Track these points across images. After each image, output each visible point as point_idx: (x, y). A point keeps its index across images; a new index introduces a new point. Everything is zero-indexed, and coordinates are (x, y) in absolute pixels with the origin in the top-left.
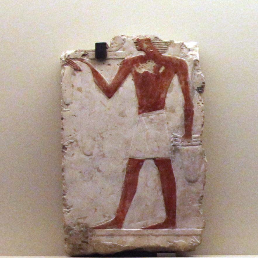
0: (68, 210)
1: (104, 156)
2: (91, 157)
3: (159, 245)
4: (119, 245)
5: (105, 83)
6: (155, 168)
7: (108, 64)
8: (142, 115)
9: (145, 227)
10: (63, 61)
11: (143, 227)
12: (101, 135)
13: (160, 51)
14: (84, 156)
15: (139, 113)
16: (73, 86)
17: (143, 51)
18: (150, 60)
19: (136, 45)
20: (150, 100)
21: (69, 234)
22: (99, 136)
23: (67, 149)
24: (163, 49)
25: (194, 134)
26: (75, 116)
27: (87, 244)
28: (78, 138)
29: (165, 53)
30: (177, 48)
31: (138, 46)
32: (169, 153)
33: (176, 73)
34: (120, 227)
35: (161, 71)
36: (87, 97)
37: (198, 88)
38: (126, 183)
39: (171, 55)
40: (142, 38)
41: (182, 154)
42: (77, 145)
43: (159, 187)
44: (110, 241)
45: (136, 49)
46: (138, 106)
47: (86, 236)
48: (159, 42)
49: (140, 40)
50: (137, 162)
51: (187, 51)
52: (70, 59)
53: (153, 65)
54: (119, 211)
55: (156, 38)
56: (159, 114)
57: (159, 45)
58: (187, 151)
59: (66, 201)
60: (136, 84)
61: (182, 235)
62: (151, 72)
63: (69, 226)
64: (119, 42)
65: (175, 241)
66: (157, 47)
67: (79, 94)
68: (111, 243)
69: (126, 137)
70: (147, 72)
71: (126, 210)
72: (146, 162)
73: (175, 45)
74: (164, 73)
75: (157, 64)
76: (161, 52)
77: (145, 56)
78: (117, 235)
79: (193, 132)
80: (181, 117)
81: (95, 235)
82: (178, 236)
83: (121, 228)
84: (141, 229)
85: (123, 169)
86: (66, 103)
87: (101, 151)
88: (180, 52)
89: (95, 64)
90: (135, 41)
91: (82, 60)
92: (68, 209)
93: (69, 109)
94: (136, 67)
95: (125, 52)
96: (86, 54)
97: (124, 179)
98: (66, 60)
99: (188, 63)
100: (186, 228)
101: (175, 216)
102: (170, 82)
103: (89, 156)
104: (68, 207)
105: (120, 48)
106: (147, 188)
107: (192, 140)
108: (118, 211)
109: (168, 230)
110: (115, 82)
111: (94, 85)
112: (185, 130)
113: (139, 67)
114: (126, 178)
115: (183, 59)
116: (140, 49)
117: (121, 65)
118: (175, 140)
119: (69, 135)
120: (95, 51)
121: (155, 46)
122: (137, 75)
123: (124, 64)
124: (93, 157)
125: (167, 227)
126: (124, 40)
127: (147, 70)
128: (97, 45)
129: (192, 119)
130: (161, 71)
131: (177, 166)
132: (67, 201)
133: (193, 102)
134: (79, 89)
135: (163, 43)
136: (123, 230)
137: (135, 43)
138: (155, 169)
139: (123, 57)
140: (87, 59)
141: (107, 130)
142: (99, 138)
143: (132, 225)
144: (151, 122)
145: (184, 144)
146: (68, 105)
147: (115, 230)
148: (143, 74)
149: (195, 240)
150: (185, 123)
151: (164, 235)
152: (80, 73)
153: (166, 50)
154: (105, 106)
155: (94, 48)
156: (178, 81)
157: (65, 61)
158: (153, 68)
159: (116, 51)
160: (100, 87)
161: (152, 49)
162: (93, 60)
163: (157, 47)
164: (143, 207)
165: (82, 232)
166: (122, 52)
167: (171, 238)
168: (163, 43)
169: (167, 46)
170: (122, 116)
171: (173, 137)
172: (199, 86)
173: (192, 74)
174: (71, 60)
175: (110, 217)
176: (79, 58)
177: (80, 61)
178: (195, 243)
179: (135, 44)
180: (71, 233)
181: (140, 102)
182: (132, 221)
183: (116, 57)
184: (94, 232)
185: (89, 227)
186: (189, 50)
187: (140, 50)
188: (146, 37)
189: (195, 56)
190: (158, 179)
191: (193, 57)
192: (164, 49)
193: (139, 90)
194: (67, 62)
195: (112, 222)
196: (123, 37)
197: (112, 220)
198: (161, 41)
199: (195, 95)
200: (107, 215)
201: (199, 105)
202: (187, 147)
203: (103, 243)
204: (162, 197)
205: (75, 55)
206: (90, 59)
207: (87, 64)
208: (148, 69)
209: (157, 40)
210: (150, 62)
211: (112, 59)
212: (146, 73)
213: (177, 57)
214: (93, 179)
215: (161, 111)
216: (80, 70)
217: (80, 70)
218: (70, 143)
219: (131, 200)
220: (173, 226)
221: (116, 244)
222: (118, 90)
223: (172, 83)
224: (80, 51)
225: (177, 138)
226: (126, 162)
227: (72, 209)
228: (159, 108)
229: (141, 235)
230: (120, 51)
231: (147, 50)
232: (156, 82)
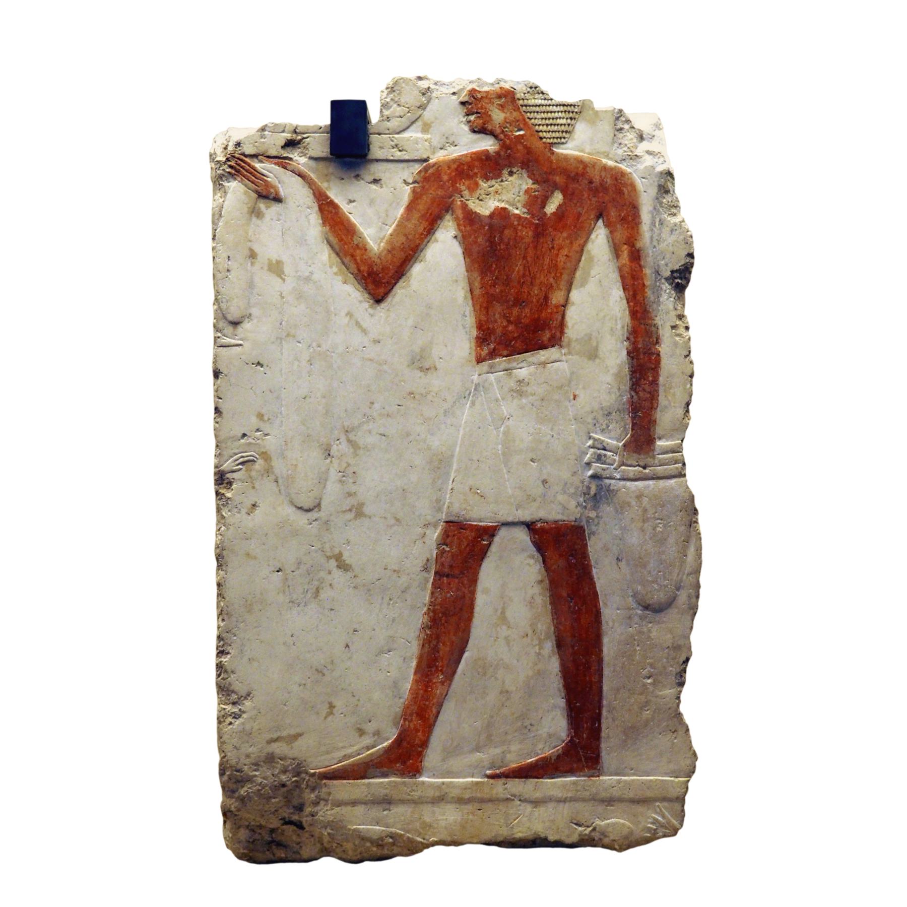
0: (235, 710)
1: (358, 511)
2: (314, 515)
3: (543, 836)
4: (408, 838)
5: (363, 248)
6: (532, 557)
7: (371, 178)
8: (491, 367)
9: (498, 772)
10: (218, 162)
11: (489, 772)
12: (352, 436)
13: (548, 135)
14: (290, 511)
15: (480, 360)
16: (253, 255)
17: (492, 133)
18: (515, 170)
19: (468, 114)
20: (515, 311)
21: (237, 795)
22: (343, 439)
23: (234, 486)
24: (556, 128)
25: (660, 439)
26: (259, 364)
27: (299, 832)
28: (271, 443)
29: (563, 143)
30: (606, 127)
31: (472, 118)
32: (579, 505)
33: (599, 216)
34: (416, 771)
35: (551, 208)
36: (300, 296)
37: (672, 272)
38: (434, 611)
39: (582, 151)
40: (486, 89)
41: (623, 507)
42: (268, 471)
43: (545, 625)
44: (378, 824)
45: (466, 128)
46: (475, 333)
47: (295, 802)
48: (543, 102)
49: (479, 96)
50: (470, 535)
51: (635, 140)
52: (242, 157)
53: (525, 187)
54: (411, 715)
55: (534, 89)
56: (544, 364)
57: (543, 115)
58: (639, 497)
59: (230, 677)
60: (467, 253)
61: (621, 800)
62: (517, 212)
63: (238, 767)
64: (411, 97)
65: (598, 822)
66: (536, 122)
67: (270, 285)
68: (383, 830)
69: (435, 442)
70: (504, 209)
71: (434, 711)
72: (503, 533)
73: (597, 115)
74: (560, 215)
75: (536, 182)
76: (551, 141)
77: (498, 153)
78: (402, 802)
79: (659, 430)
80: (618, 375)
81: (326, 801)
82: (610, 801)
83: (414, 776)
84: (486, 780)
85: (425, 561)
86: (230, 318)
87: (349, 494)
88: (613, 142)
89: (326, 177)
90: (462, 99)
91: (282, 161)
92: (234, 703)
93: (241, 340)
94: (466, 193)
95: (429, 136)
96: (299, 142)
97: (427, 599)
98: (228, 160)
99: (640, 184)
100: (634, 775)
101: (599, 729)
102: (582, 250)
103: (309, 510)
104: (234, 697)
105: (413, 123)
106: (504, 627)
107: (654, 457)
108: (406, 715)
109: (574, 783)
110: (398, 245)
111: (325, 255)
112: (634, 424)
113: (479, 192)
114: (432, 593)
115: (623, 166)
116: (425, 224)
117: (416, 185)
118: (599, 458)
119: (240, 435)
120: (329, 130)
121: (531, 119)
122: (470, 219)
123: (426, 179)
124: (322, 514)
125: (570, 772)
126: (426, 92)
127: (503, 205)
128: (338, 107)
129: (655, 382)
130: (551, 208)
131: (606, 549)
132: (232, 676)
133: (658, 321)
134: (276, 268)
135: (555, 108)
136: (423, 783)
137: (463, 103)
138: (532, 562)
139: (425, 156)
140: (303, 160)
141: (368, 418)
142: (344, 447)
143: (456, 763)
144: (521, 394)
145: (628, 471)
146: (235, 324)
147: (395, 782)
148: (492, 216)
149: (664, 817)
150: (632, 397)
151: (564, 801)
152: (275, 208)
153: (566, 132)
154: (364, 331)
155: (325, 119)
156: (605, 241)
157: (225, 163)
158: (523, 198)
159: (398, 133)
160: (347, 260)
161: (520, 130)
162: (321, 165)
163: (537, 119)
164: (492, 697)
165: (284, 789)
166: (419, 135)
167: (585, 810)
168: (555, 108)
169: (571, 119)
170: (421, 369)
171: (590, 447)
172: (676, 267)
173: (653, 224)
174: (247, 160)
175: (377, 733)
176: (273, 152)
177: (275, 164)
178: (662, 826)
179: (462, 110)
180: (242, 792)
181: (483, 318)
182: (451, 751)
183: (399, 153)
184: (324, 790)
185: (307, 773)
186: (641, 138)
187: (481, 130)
188: (497, 86)
189: (662, 160)
190: (539, 596)
191: (656, 160)
192: (559, 128)
193: (476, 275)
194: (231, 167)
195: (388, 750)
196: (424, 84)
197: (386, 744)
198: (551, 99)
199: (664, 297)
200: (370, 727)
201: (678, 332)
202: (640, 484)
203: (354, 830)
204: (554, 665)
205: (261, 143)
206: (311, 158)
207: (301, 175)
208: (508, 202)
209: (536, 96)
210: (515, 176)
211: (387, 161)
212: (501, 214)
213: (604, 161)
214: (323, 595)
215: (552, 353)
216: (278, 199)
217: (278, 199)
218: (242, 463)
219: (451, 676)
220: (589, 768)
221: (397, 834)
222: (408, 274)
223: (589, 251)
224: (278, 128)
225: (604, 449)
226: (435, 534)
227: (248, 703)
228: (546, 342)
229: (482, 801)
230: (413, 134)
231: (503, 132)
232: (535, 247)
